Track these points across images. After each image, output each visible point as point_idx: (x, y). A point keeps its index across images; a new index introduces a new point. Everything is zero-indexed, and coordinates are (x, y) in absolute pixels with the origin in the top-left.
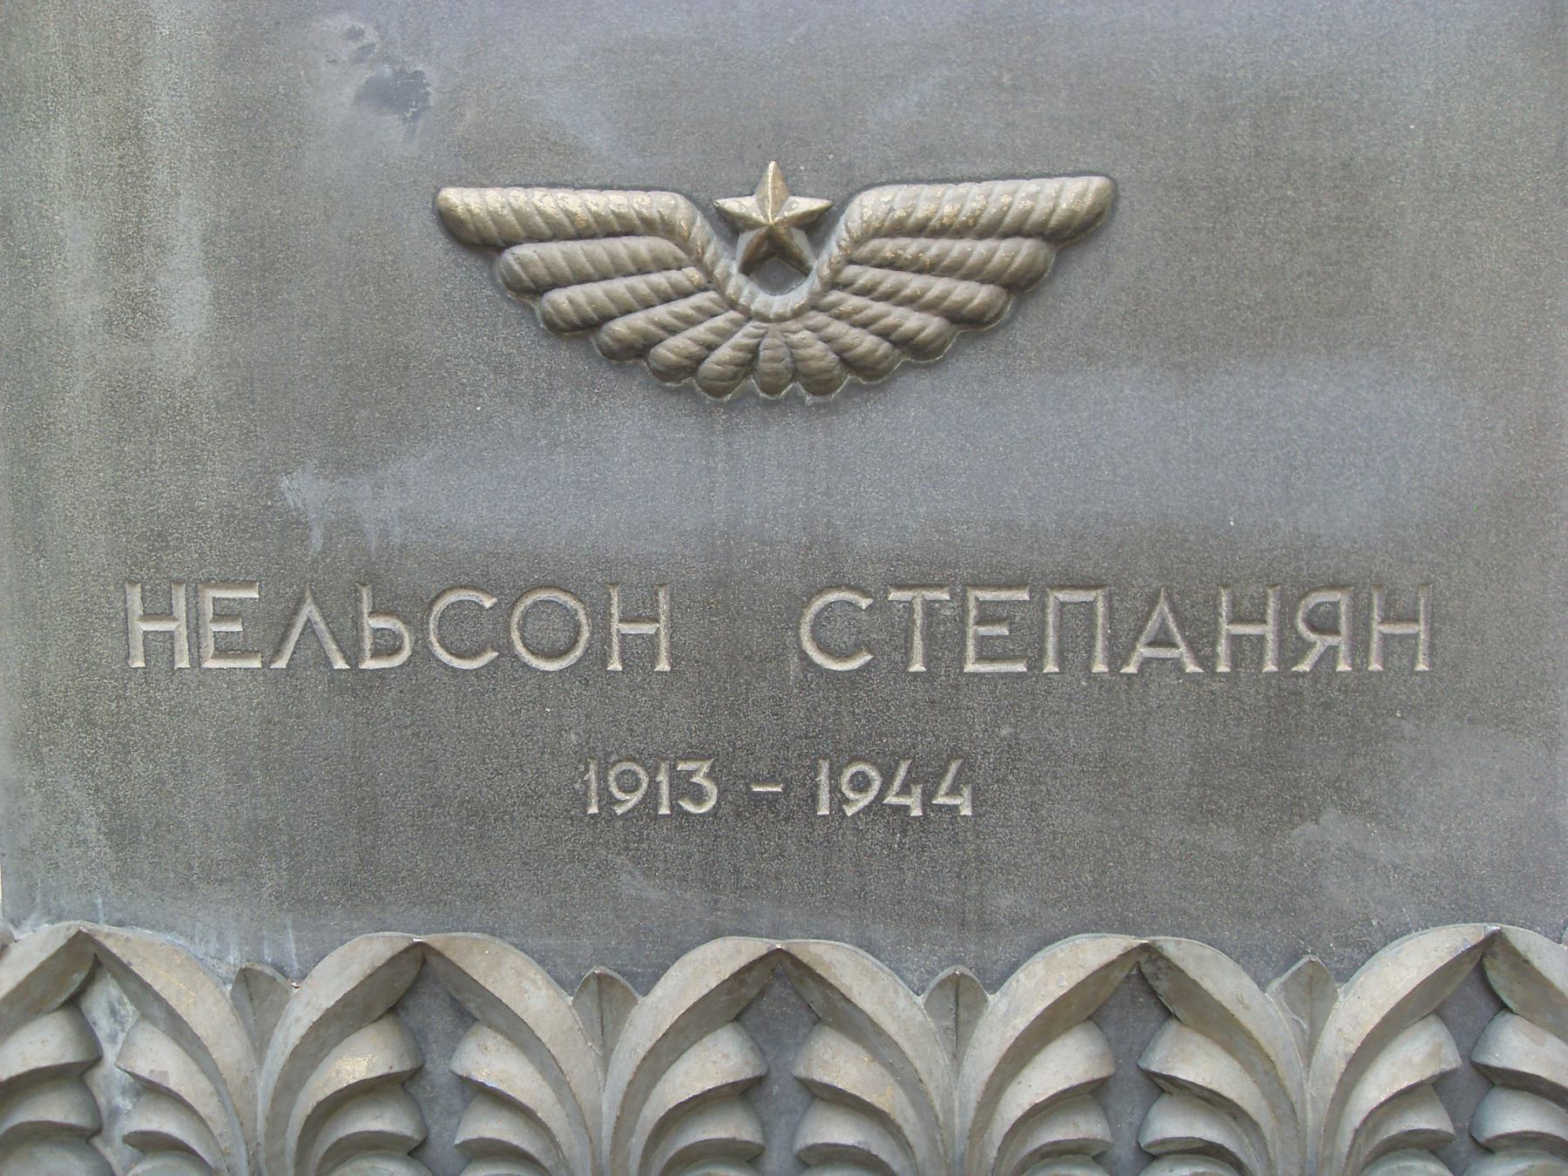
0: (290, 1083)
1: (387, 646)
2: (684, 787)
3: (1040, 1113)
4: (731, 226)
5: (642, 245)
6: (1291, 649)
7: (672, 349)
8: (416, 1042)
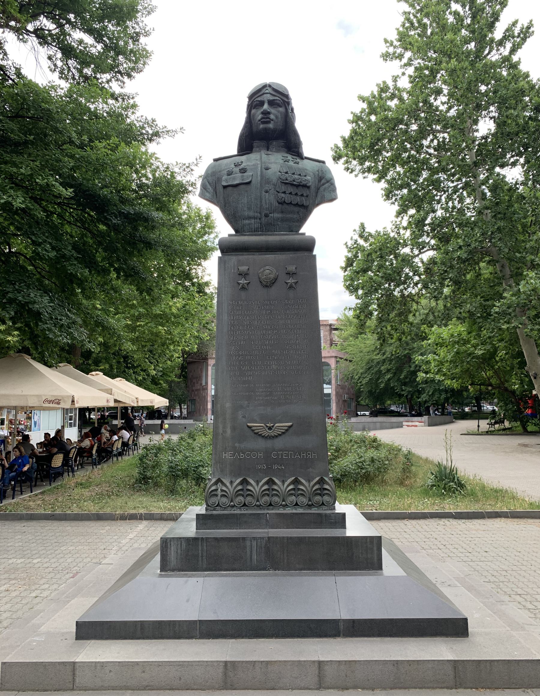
0: (234, 490)
1: (242, 456)
2: (264, 467)
3: (289, 491)
4: (267, 426)
6: (307, 456)
7: (263, 435)
8: (244, 486)
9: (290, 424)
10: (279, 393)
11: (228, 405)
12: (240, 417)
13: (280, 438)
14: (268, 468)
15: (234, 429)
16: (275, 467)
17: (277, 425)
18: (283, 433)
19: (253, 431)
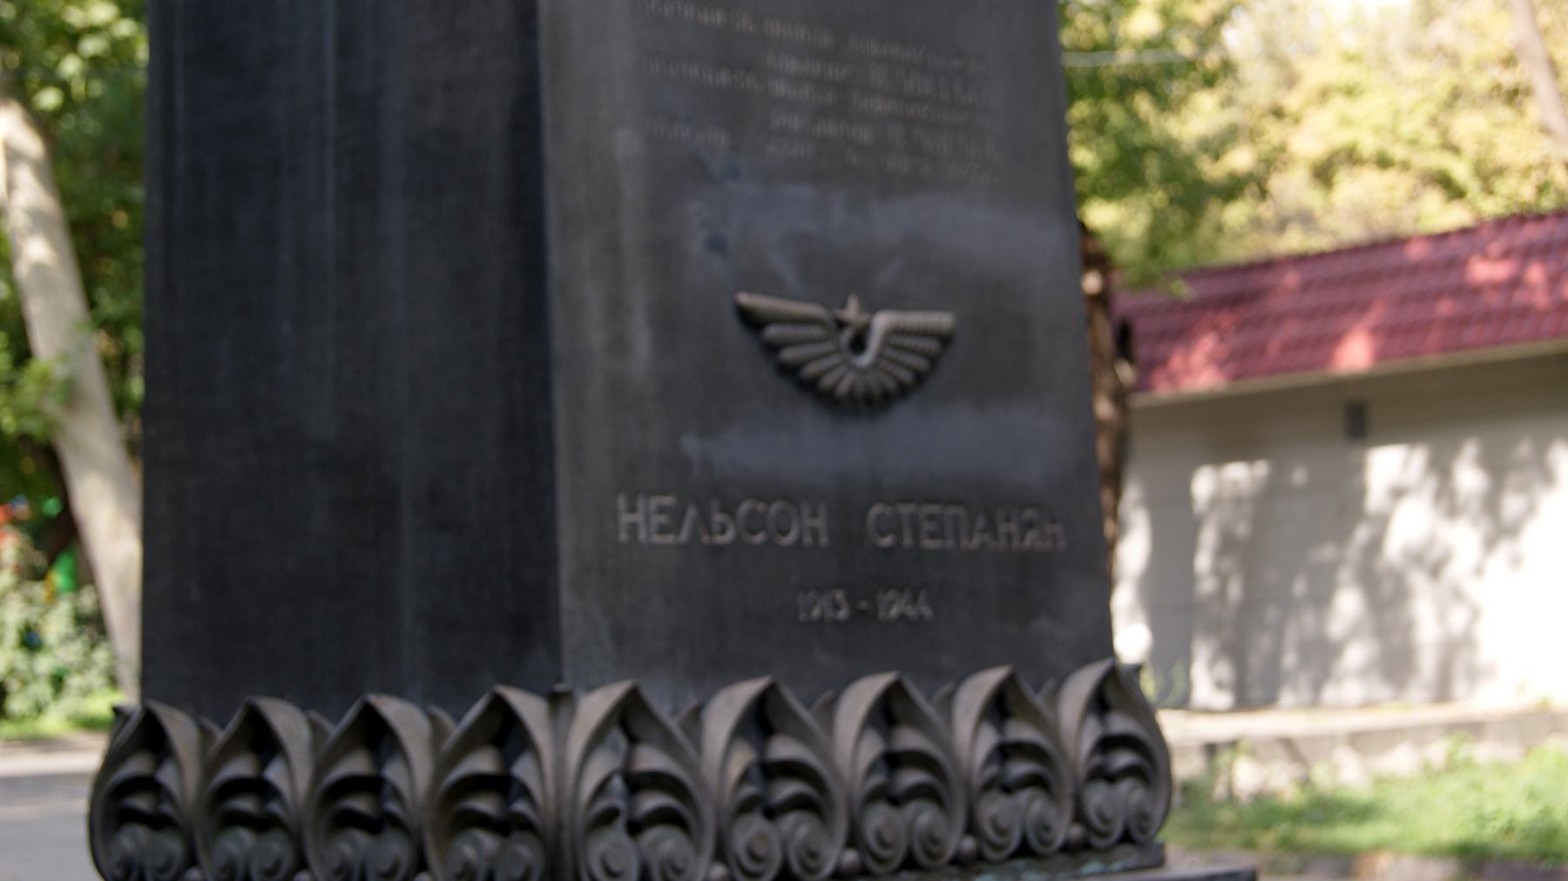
5: (814, 331)
7: (827, 382)
9: (941, 320)
10: (879, 106)
11: (626, 143)
12: (696, 245)
13: (902, 417)
14: (856, 614)
15: (667, 324)
16: (895, 607)
17: (882, 321)
18: (920, 378)
19: (772, 348)
